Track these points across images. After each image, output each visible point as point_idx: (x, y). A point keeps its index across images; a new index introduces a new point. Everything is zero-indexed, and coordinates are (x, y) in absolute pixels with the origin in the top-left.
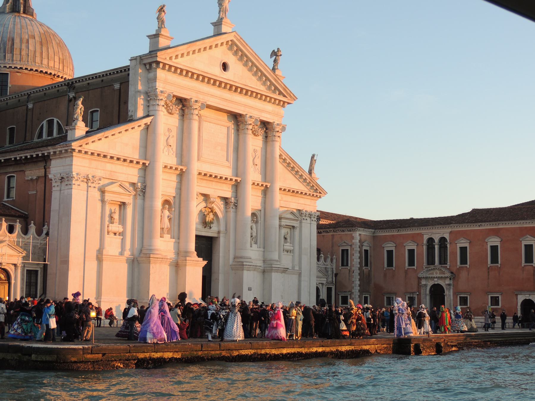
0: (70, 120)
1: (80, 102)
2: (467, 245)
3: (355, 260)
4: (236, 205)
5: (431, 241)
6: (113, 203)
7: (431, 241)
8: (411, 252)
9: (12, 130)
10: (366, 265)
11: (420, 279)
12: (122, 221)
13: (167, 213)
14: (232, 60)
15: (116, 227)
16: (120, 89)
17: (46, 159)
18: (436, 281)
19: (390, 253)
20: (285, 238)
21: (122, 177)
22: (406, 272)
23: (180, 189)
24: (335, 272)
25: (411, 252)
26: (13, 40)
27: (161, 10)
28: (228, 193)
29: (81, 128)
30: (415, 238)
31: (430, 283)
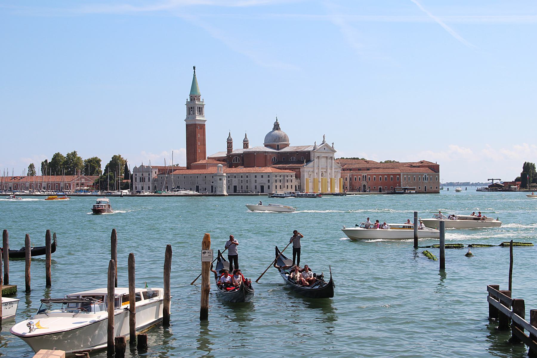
2: (370, 177)
3: (348, 180)
4: (327, 172)
5: (363, 176)
7: (363, 176)
8: (360, 178)
9: (284, 158)
10: (351, 180)
16: (307, 154)
17: (300, 168)
18: (364, 184)
19: (355, 178)
22: (359, 182)
25: (360, 178)
27: (315, 142)
31: (363, 184)
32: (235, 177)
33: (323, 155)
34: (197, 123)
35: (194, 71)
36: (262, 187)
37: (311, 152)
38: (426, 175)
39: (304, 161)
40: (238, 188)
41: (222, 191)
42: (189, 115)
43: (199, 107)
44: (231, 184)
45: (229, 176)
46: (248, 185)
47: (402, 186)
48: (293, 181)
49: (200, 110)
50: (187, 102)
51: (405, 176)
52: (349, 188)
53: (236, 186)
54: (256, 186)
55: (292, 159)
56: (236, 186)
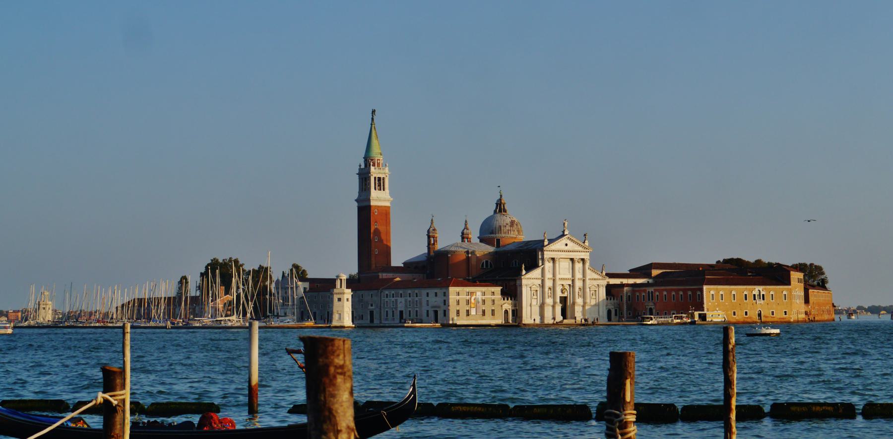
0: (522, 271)
1: (523, 265)
4: (573, 286)
5: (649, 292)
6: (534, 290)
7: (649, 292)
8: (644, 296)
11: (646, 306)
12: (537, 295)
13: (550, 291)
14: (569, 242)
15: (535, 297)
17: (515, 280)
18: (650, 307)
19: (638, 296)
20: (592, 294)
21: (535, 283)
23: (553, 284)
24: (618, 303)
26: (501, 226)
28: (570, 283)
29: (524, 272)
30: (645, 291)
31: (649, 307)
32: (401, 297)
33: (564, 255)
34: (373, 203)
35: (373, 119)
36: (436, 312)
37: (537, 250)
38: (761, 290)
39: (522, 267)
40: (405, 314)
41: (340, 318)
42: (362, 191)
43: (378, 178)
44: (396, 308)
45: (393, 294)
46: (418, 309)
47: (705, 309)
48: (495, 302)
49: (380, 183)
50: (359, 169)
51: (712, 292)
52: (627, 314)
53: (403, 311)
54: (428, 311)
55: (514, 263)
56: (403, 311)
